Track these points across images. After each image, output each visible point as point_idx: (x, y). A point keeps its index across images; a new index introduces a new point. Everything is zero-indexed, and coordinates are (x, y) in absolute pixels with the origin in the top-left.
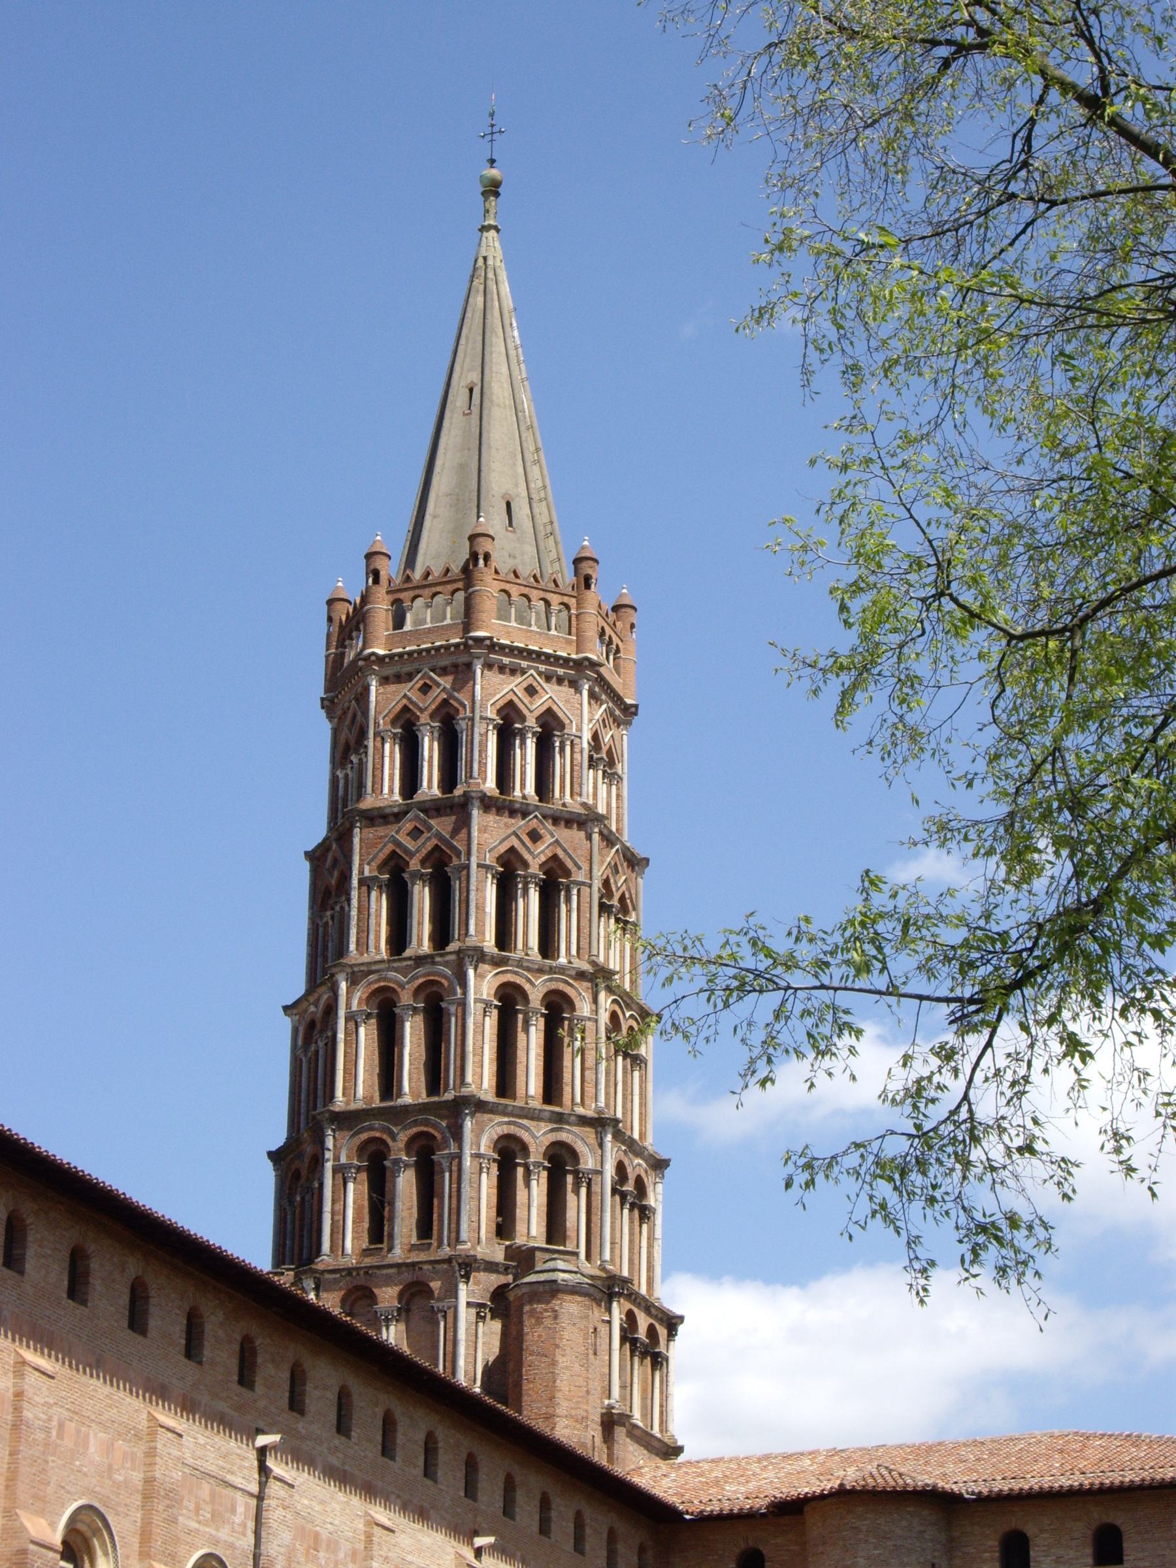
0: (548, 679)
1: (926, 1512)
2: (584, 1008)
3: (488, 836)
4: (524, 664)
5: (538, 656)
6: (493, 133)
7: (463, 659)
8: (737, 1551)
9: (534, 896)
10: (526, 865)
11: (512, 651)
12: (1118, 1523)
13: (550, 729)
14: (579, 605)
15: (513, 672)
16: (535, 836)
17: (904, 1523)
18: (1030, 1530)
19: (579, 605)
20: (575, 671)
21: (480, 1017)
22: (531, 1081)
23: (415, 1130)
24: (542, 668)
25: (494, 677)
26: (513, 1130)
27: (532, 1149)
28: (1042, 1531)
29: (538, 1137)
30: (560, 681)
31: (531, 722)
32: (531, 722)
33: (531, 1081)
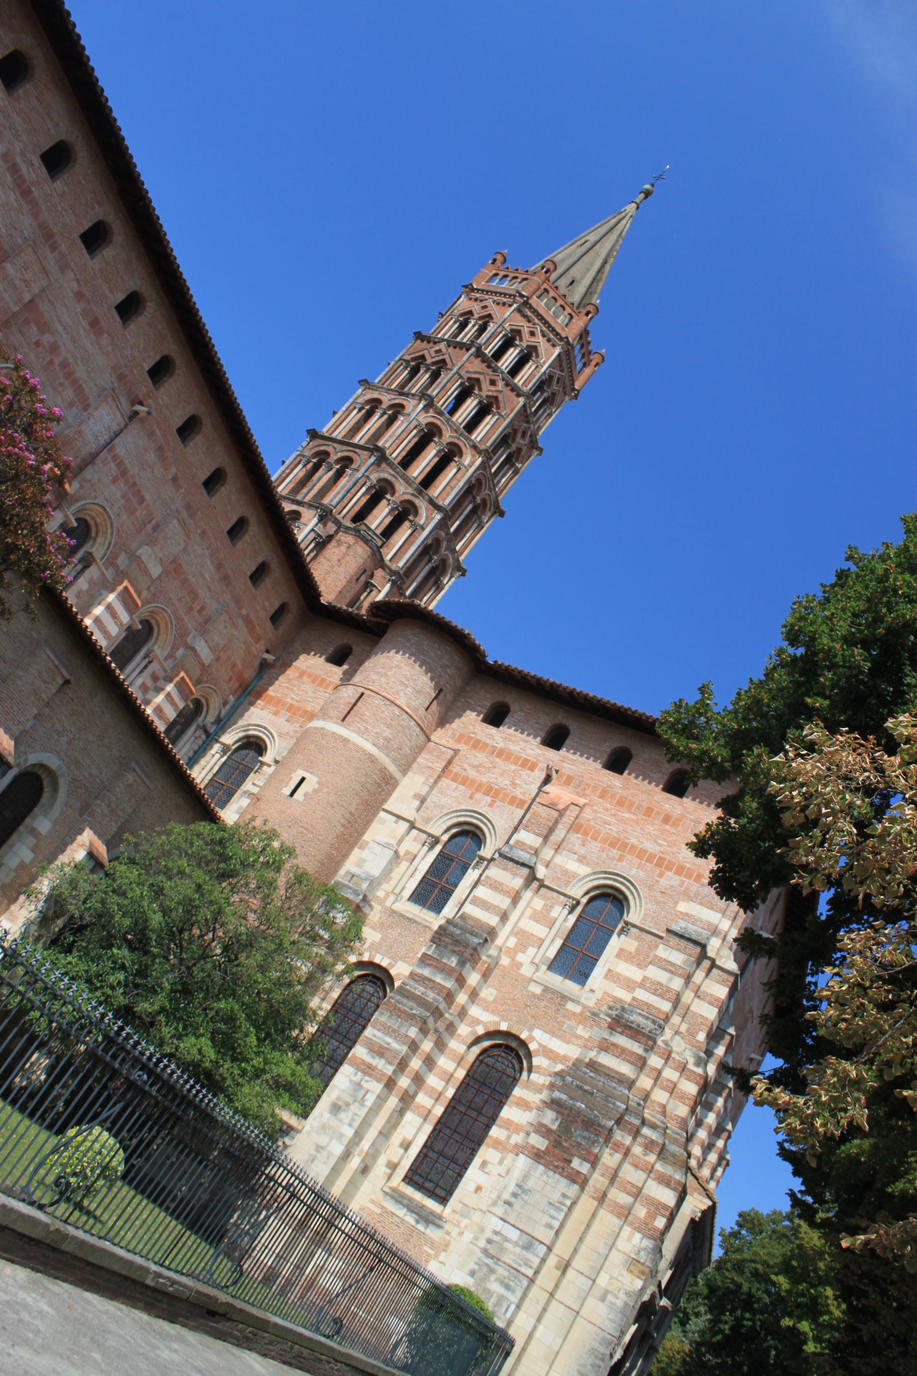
0: (544, 336)
1: (457, 658)
2: (467, 460)
4: (537, 321)
5: (546, 322)
8: (340, 642)
11: (535, 312)
12: (571, 728)
15: (529, 321)
17: (439, 652)
18: (514, 707)
21: (412, 426)
22: (419, 469)
23: (346, 454)
24: (544, 329)
25: (518, 316)
26: (393, 479)
27: (397, 495)
28: (521, 711)
30: (549, 340)
31: (524, 344)
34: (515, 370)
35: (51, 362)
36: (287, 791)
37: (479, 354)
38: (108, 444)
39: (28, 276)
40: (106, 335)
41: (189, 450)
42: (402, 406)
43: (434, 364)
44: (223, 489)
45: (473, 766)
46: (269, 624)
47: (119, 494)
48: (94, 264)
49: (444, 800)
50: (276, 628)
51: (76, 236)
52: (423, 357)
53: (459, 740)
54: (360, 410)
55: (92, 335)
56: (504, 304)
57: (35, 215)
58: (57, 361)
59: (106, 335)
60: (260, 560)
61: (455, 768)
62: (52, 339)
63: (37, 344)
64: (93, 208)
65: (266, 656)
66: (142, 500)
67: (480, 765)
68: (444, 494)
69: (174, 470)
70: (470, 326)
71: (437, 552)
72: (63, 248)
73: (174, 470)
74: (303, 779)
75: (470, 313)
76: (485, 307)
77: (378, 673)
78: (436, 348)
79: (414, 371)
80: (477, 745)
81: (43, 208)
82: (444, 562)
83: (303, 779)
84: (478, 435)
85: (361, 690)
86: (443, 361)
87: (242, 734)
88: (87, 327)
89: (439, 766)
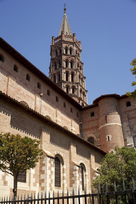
2: (75, 73)
3: (64, 57)
6: (65, 5)
7: (61, 43)
9: (70, 64)
10: (68, 60)
13: (71, 50)
14: (73, 38)
16: (69, 58)
18: (130, 101)
19: (73, 38)
20: (73, 43)
25: (64, 44)
29: (71, 85)
31: (69, 48)
32: (69, 48)
33: (70, 80)
34: (71, 53)
35: (25, 96)
36: (108, 140)
37: (64, 55)
38: (41, 105)
39: (12, 82)
40: (28, 85)
41: (51, 97)
42: (59, 72)
43: (58, 62)
44: (59, 100)
45: (132, 115)
46: (77, 118)
47: (47, 112)
48: (19, 74)
49: (132, 124)
50: (78, 117)
51: (13, 70)
52: (55, 62)
53: (126, 112)
54: (53, 77)
55: (27, 87)
56: (61, 44)
57: (5, 71)
58: (25, 95)
59: (28, 85)
60: (70, 108)
61: (130, 117)
62: (22, 92)
63: (21, 94)
64: (12, 63)
65: (80, 123)
66: (51, 110)
67: (133, 114)
68: (77, 81)
69: (51, 102)
70: (58, 52)
71: (82, 91)
72: (13, 74)
73: (51, 102)
74: (109, 137)
75: (56, 49)
76: (58, 47)
77: (105, 111)
78: (56, 59)
79: (56, 65)
80: (129, 111)
81: (6, 69)
82: (84, 91)
83: (109, 137)
84: (74, 67)
85: (105, 116)
86: (59, 60)
87: (87, 138)
88: (25, 86)
89: (127, 119)
